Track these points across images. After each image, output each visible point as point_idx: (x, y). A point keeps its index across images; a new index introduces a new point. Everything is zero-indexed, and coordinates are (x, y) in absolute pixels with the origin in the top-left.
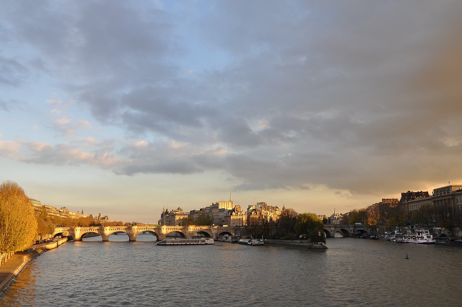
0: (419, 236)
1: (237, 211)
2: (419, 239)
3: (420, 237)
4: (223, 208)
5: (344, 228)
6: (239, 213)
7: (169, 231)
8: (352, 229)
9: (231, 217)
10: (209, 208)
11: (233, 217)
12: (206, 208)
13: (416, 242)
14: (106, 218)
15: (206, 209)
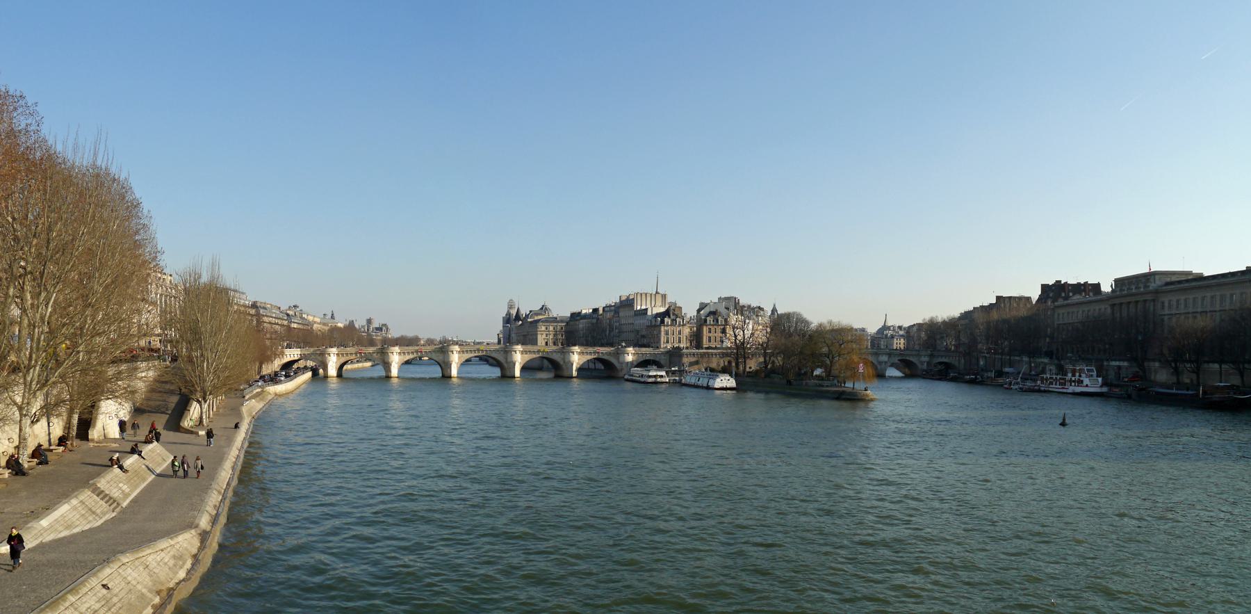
0: (1073, 379)
1: (674, 314)
2: (1073, 384)
3: (1074, 381)
4: (644, 307)
5: (908, 358)
6: (678, 319)
7: (528, 357)
8: (926, 359)
9: (662, 328)
10: (613, 308)
11: (666, 328)
12: (607, 307)
13: (1065, 391)
14: (384, 328)
15: (606, 309)
